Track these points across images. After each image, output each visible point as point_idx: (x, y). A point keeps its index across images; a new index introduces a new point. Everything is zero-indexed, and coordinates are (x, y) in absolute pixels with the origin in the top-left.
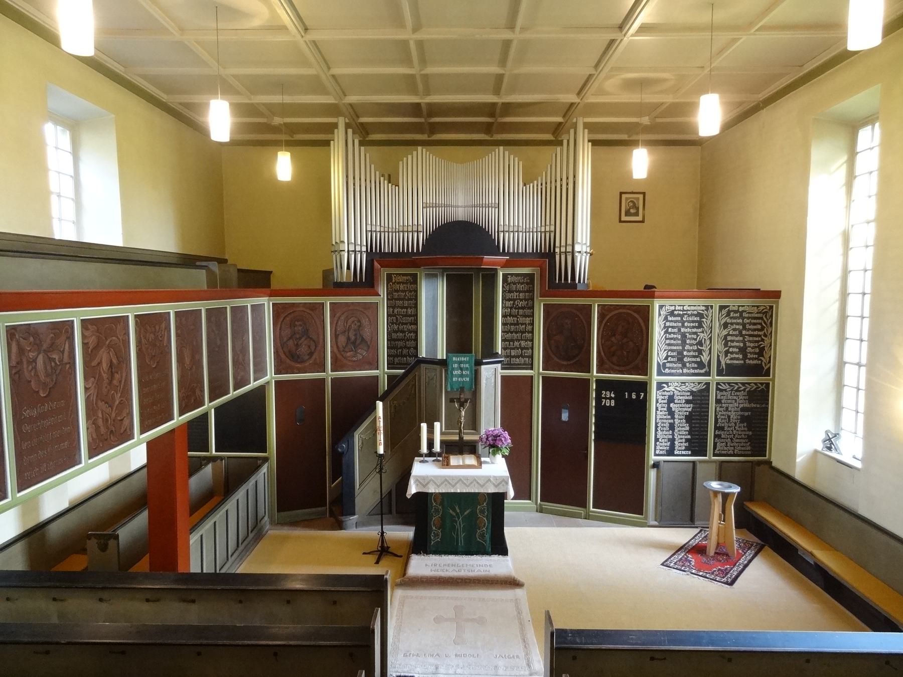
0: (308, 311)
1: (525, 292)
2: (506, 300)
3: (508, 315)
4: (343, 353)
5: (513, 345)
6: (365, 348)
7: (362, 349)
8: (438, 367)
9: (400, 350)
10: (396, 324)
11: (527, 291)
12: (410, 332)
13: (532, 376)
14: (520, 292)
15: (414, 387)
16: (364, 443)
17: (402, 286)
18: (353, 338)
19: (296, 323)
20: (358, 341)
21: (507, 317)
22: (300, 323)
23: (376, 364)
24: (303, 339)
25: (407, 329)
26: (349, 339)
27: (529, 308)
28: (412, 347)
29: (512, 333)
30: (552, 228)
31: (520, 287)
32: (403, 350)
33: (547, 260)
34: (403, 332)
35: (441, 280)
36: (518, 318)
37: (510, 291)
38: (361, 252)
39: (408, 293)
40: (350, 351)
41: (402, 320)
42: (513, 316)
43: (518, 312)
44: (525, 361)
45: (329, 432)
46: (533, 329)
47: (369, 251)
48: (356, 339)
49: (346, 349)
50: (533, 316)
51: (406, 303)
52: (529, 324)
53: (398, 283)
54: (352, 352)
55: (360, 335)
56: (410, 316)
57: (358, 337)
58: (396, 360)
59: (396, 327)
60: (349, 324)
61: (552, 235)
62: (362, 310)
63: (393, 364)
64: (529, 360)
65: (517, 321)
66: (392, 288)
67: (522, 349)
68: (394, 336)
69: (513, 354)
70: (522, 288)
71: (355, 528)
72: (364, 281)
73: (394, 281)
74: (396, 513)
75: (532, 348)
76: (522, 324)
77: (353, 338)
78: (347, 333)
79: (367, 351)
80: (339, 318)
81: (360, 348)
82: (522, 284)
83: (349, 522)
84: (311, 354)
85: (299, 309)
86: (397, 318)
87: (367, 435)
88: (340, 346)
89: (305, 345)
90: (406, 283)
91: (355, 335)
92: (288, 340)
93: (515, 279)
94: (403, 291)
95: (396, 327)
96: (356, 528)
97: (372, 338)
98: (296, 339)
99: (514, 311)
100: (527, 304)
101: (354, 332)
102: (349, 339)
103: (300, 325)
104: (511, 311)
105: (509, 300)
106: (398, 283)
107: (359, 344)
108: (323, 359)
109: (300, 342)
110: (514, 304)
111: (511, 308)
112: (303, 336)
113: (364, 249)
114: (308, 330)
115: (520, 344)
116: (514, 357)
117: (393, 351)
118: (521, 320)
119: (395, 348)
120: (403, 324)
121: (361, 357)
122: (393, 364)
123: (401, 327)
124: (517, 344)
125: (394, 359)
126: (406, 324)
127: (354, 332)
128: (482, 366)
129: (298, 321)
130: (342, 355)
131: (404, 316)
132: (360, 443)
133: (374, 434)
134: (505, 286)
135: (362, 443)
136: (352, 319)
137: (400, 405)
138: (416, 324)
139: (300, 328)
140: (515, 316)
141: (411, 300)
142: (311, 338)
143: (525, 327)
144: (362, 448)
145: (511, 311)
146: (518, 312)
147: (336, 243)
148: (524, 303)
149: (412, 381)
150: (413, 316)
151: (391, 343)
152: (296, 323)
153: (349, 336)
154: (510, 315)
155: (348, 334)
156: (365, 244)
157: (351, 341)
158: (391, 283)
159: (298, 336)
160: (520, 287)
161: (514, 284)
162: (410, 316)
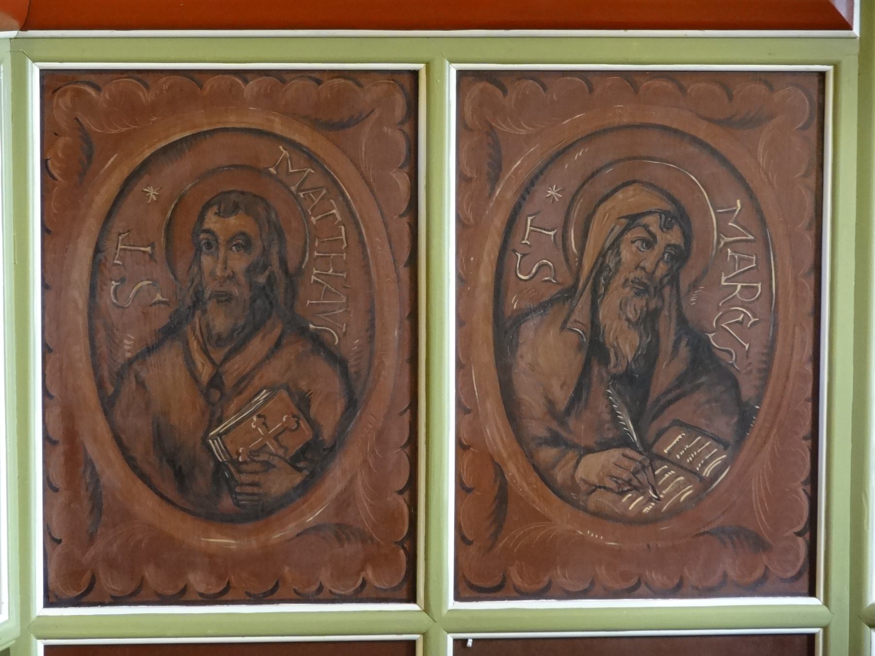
0: (303, 136)
4: (548, 454)
6: (725, 426)
7: (693, 430)
19: (212, 222)
22: (234, 222)
23: (802, 545)
24: (258, 347)
40: (605, 446)
54: (614, 455)
55: (682, 320)
62: (702, 131)
80: (527, 190)
81: (681, 425)
85: (233, 120)
89: (273, 389)
92: (150, 350)
98: (210, 341)
101: (640, 302)
109: (237, 366)
112: (256, 328)
121: (688, 492)
127: (640, 302)
130: (544, 476)
139: (239, 263)
142: (318, 342)
152: (212, 222)
157: (616, 366)
159: (220, 323)
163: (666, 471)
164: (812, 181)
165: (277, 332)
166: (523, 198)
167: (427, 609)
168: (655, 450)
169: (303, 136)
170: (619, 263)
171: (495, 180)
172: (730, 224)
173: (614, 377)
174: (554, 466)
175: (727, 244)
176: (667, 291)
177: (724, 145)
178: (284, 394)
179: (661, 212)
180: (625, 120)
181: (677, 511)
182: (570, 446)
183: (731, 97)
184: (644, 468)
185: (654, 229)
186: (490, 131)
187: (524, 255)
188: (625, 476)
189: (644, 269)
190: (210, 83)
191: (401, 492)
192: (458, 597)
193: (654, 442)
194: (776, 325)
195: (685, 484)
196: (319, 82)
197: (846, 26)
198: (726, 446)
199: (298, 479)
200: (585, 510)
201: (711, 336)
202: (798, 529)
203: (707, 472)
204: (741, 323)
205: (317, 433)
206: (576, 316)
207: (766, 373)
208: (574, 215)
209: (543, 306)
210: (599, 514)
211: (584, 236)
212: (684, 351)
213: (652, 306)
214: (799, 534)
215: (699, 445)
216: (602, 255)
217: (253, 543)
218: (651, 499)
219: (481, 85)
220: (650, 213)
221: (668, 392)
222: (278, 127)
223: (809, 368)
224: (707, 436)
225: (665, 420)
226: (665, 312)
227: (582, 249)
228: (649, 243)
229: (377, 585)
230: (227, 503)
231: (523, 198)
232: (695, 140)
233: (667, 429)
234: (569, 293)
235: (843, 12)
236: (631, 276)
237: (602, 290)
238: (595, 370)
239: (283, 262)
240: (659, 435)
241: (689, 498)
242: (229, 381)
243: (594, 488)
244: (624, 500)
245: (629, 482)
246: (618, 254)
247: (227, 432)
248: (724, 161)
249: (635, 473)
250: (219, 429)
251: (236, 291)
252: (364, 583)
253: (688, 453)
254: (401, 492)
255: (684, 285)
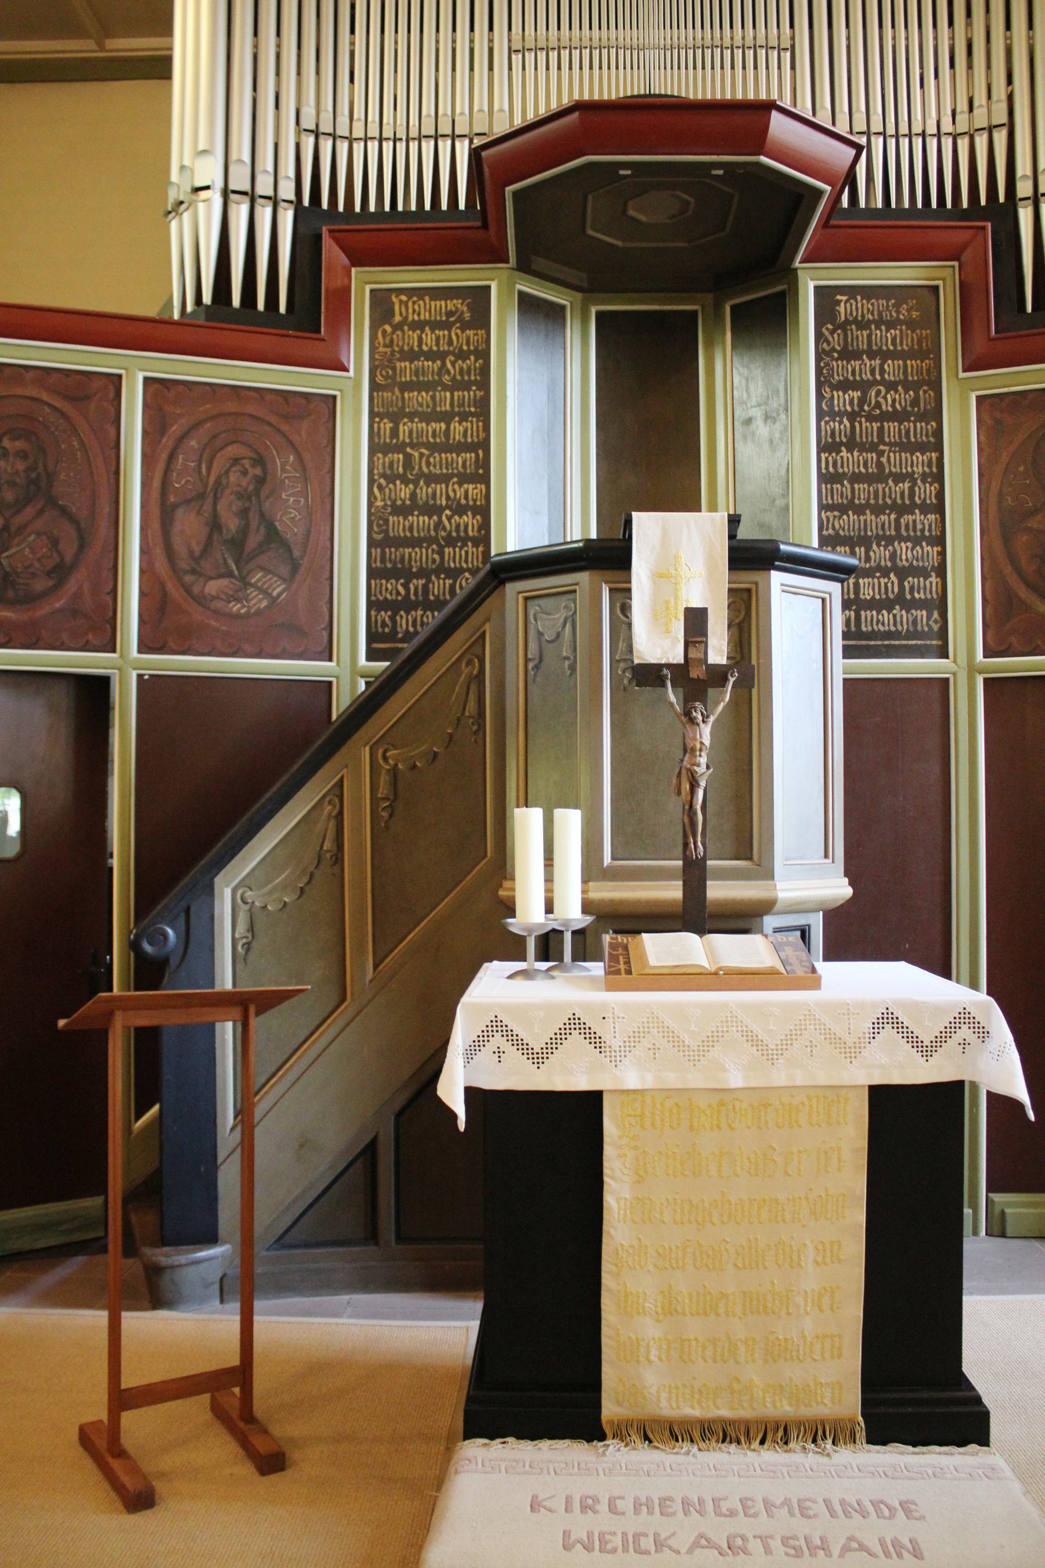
0: (58, 403)
1: (903, 356)
2: (834, 387)
3: (841, 443)
4: (188, 579)
5: (868, 559)
6: (284, 570)
7: (267, 571)
8: (583, 578)
9: (421, 582)
10: (406, 482)
11: (910, 355)
12: (460, 510)
13: (947, 679)
14: (886, 356)
15: (473, 688)
16: (258, 927)
17: (429, 338)
18: (232, 524)
19: (6, 443)
20: (254, 540)
21: (839, 451)
22: (19, 444)
23: (325, 634)
24: (29, 511)
25: (448, 498)
26: (215, 525)
27: (922, 417)
28: (468, 570)
29: (859, 510)
30: (1000, 116)
31: (886, 338)
32: (429, 581)
33: (989, 225)
34: (431, 509)
35: (577, 327)
36: (881, 454)
37: (848, 354)
38: (275, 201)
39: (453, 364)
40: (220, 576)
41: (428, 464)
42: (863, 448)
43: (881, 430)
44: (915, 622)
45: (125, 897)
46: (940, 495)
47: (306, 202)
48: (244, 531)
49: (206, 566)
50: (939, 447)
51: (446, 400)
52: (924, 477)
53: (419, 326)
54: (224, 582)
55: (262, 515)
56: (461, 448)
57: (254, 520)
58: (404, 622)
59: (404, 492)
60: (218, 465)
61: (1000, 138)
62: (273, 419)
63: (392, 637)
64: (929, 618)
65: (879, 464)
66: (391, 345)
67: (902, 574)
68: (398, 525)
69: (866, 594)
70: (894, 340)
71: (217, 1302)
72: (282, 309)
73: (397, 318)
74: (397, 1243)
75: (941, 571)
76: (899, 478)
77: (232, 524)
78: (209, 501)
79: (289, 580)
80: (180, 440)
82: (891, 325)
83: (191, 1272)
84: (61, 572)
85: (19, 391)
86: (408, 458)
87: (271, 893)
88: (181, 550)
89: (39, 534)
90: (446, 326)
91: (244, 513)
93: (861, 307)
94: (430, 356)
95: (404, 492)
96: (222, 1301)
97: (309, 532)
99: (867, 428)
100: (915, 402)
102: (215, 525)
103: (23, 455)
104: (853, 427)
105: (845, 386)
106: (419, 326)
107: (262, 548)
108: (109, 599)
109: (18, 520)
110: (862, 401)
111: (852, 416)
112: (28, 500)
113: (287, 191)
114: (51, 476)
115: (893, 556)
116: (873, 604)
117: (393, 589)
118: (894, 461)
119: (401, 572)
120: (431, 479)
121: (264, 604)
122: (392, 637)
123: (424, 492)
124: (880, 554)
125: (393, 618)
126: (445, 479)
127: (240, 504)
128: (774, 573)
129: (16, 434)
130: (188, 590)
131: (434, 448)
132: (242, 928)
133: (302, 889)
134: (827, 333)
135: (251, 928)
136: (233, 450)
137: (414, 767)
138: (485, 479)
139: (21, 466)
140: (873, 448)
141: (466, 386)
142: (64, 511)
143: (912, 490)
144: (248, 947)
145: (853, 427)
146: (881, 430)
147: (183, 168)
148: (901, 398)
149: (469, 663)
150: (472, 448)
151: (383, 553)
152: (6, 443)
153: (215, 515)
154: (851, 445)
155: (215, 504)
156: (292, 173)
158: (388, 328)
160: (886, 338)
161: (863, 325)
162: (461, 448)
163: (252, 592)
164: (329, 450)
165: (39, 506)
166: (177, 445)
167: (121, 656)
168: (247, 580)
169: (58, 403)
170: (228, 483)
171: (163, 434)
172: (288, 467)
173: (226, 541)
174: (192, 584)
175: (286, 478)
176: (253, 498)
177: (284, 428)
178: (44, 537)
179: (251, 458)
180: (233, 410)
181: (259, 612)
182: (201, 575)
183: (287, 403)
184: (241, 590)
185: (247, 466)
186: (160, 409)
187: (178, 474)
188: (231, 593)
189: (241, 486)
190: (7, 371)
191: (108, 594)
192: (140, 651)
193: (247, 575)
194: (311, 521)
195: (262, 599)
196: (67, 376)
197: (347, 370)
198: (285, 580)
199: (51, 583)
200: (209, 609)
201: (277, 523)
202: (323, 626)
203: (275, 594)
204: (293, 518)
205: (62, 559)
206: (205, 508)
207: (305, 545)
208: (205, 456)
209: (188, 502)
210: (215, 611)
211: (209, 469)
212: (262, 529)
213: (247, 504)
214: (324, 629)
215: (271, 579)
216: (219, 477)
217: (25, 617)
218: (245, 606)
219: (156, 386)
220: (244, 458)
221: (254, 550)
222: (45, 397)
223: (328, 543)
224: (275, 575)
225: (252, 565)
226: (253, 509)
227: (209, 469)
228: (245, 473)
229: (94, 642)
230: (10, 594)
231: (177, 445)
232: (269, 424)
233: (253, 570)
234: (201, 496)
235: (346, 365)
236: (235, 489)
237: (219, 495)
238: (215, 537)
239: (45, 467)
240: (249, 572)
241: (265, 607)
242: (13, 529)
243: (214, 598)
244: (231, 605)
245: (232, 596)
246: (228, 478)
247: (11, 556)
248: (284, 435)
249: (237, 591)
250: (6, 554)
251: (18, 480)
252: (87, 642)
253: (265, 583)
254: (108, 594)
255: (262, 498)
